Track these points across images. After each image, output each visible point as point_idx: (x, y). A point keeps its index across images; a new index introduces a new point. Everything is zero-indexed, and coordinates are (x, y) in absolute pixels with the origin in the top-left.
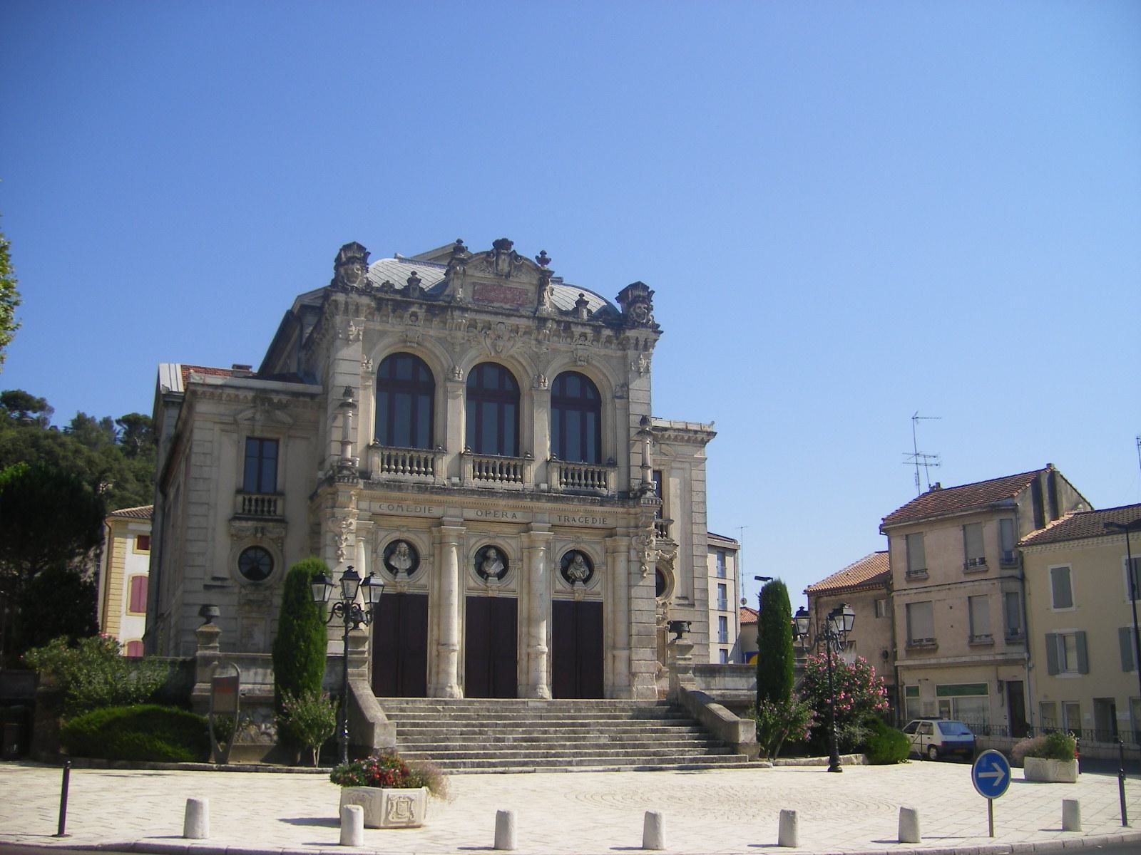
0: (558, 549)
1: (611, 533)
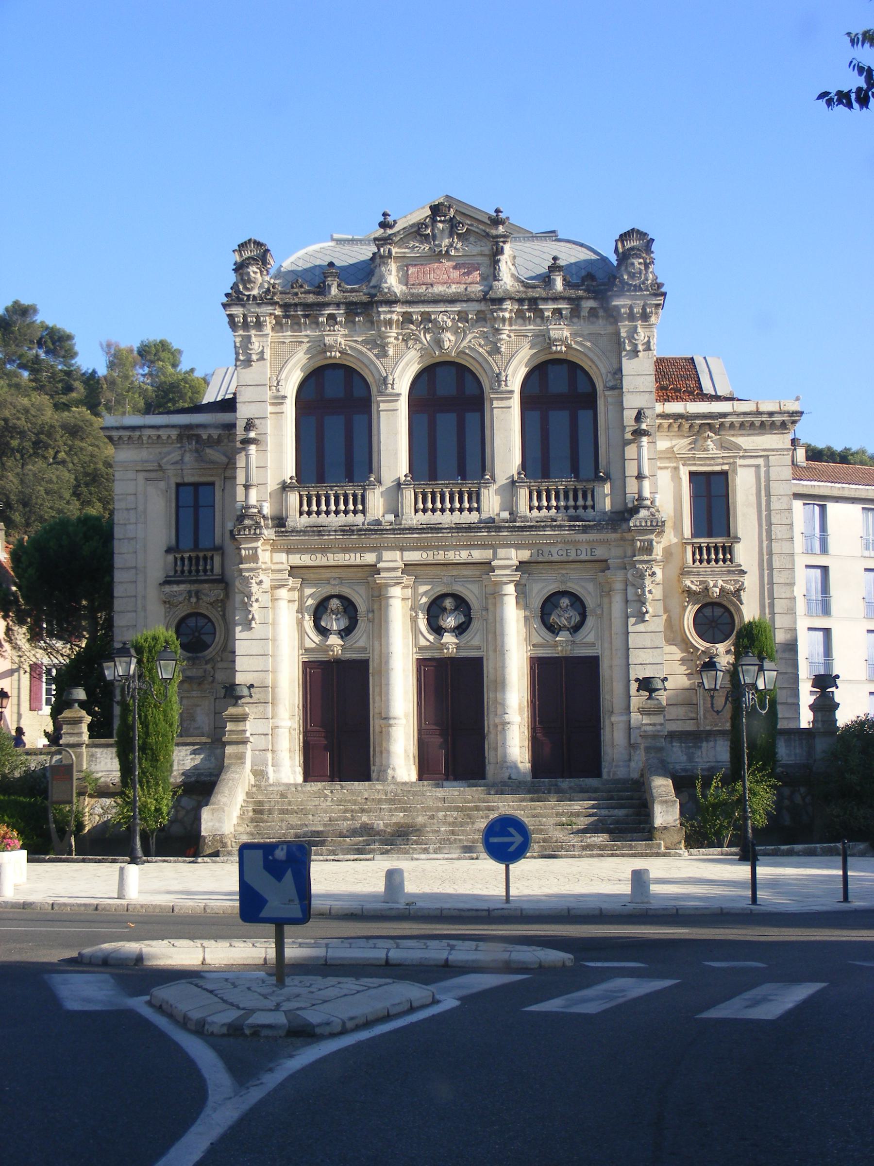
0: (535, 591)
1: (603, 565)
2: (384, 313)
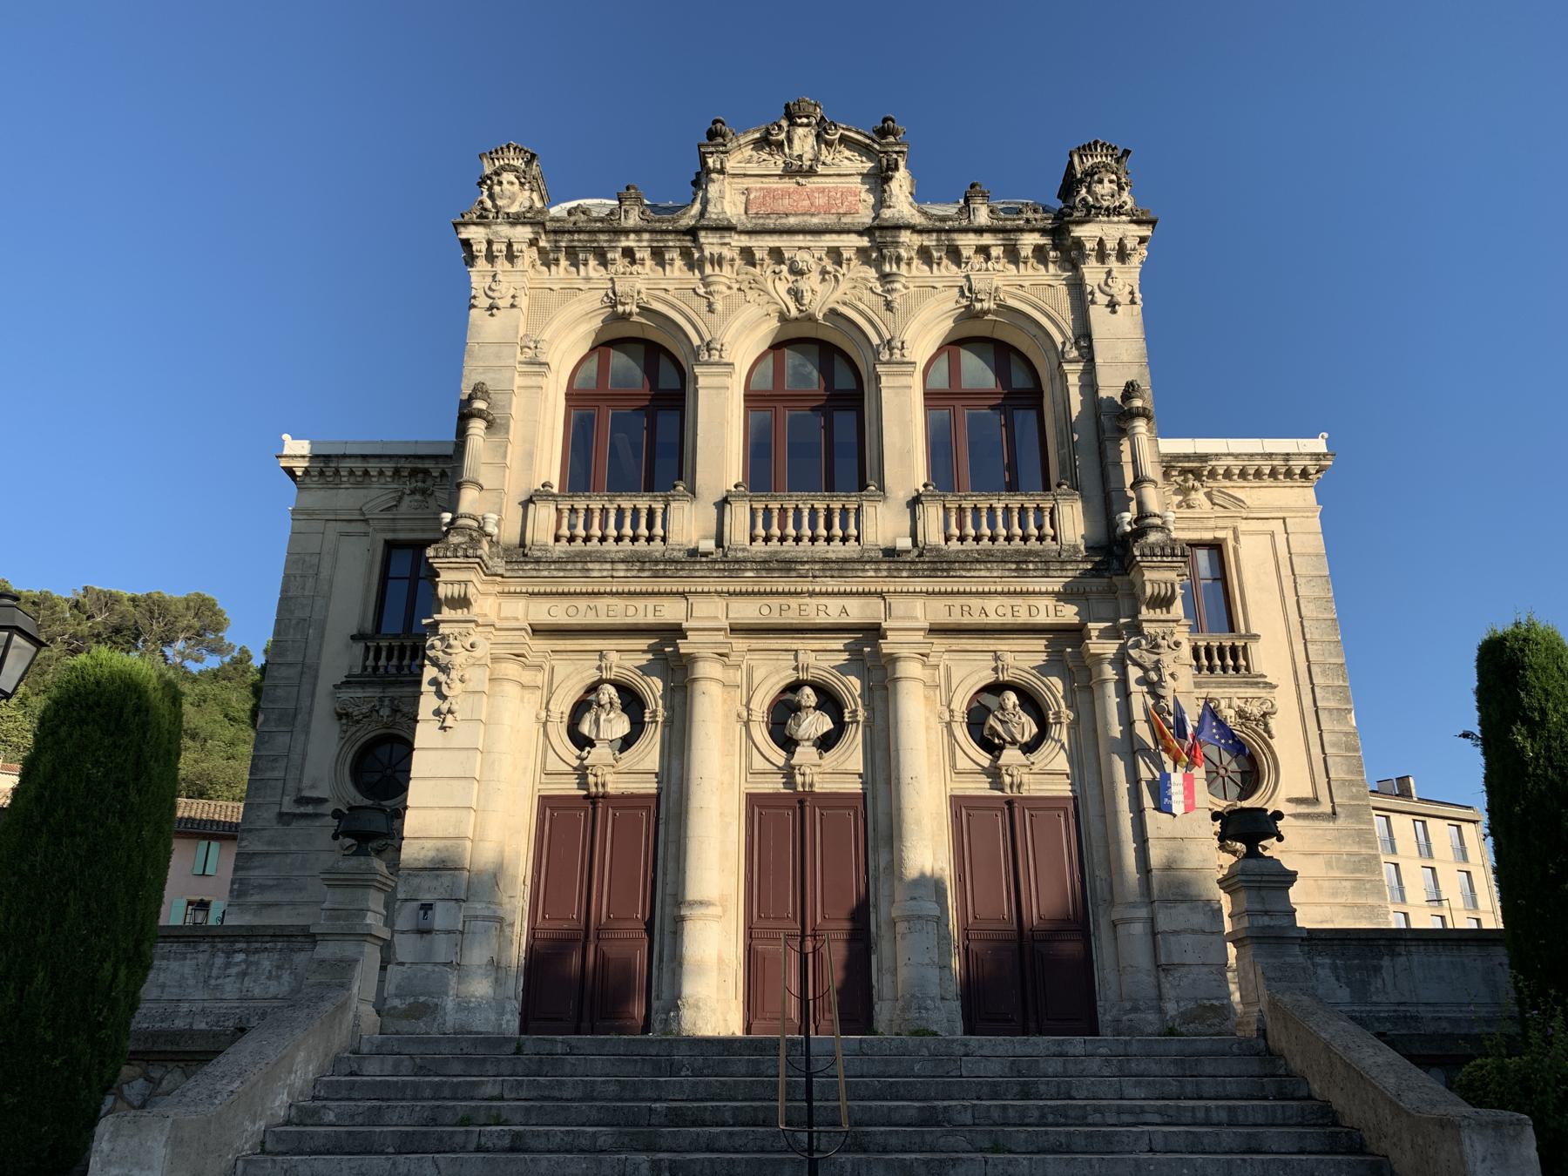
2: (710, 244)
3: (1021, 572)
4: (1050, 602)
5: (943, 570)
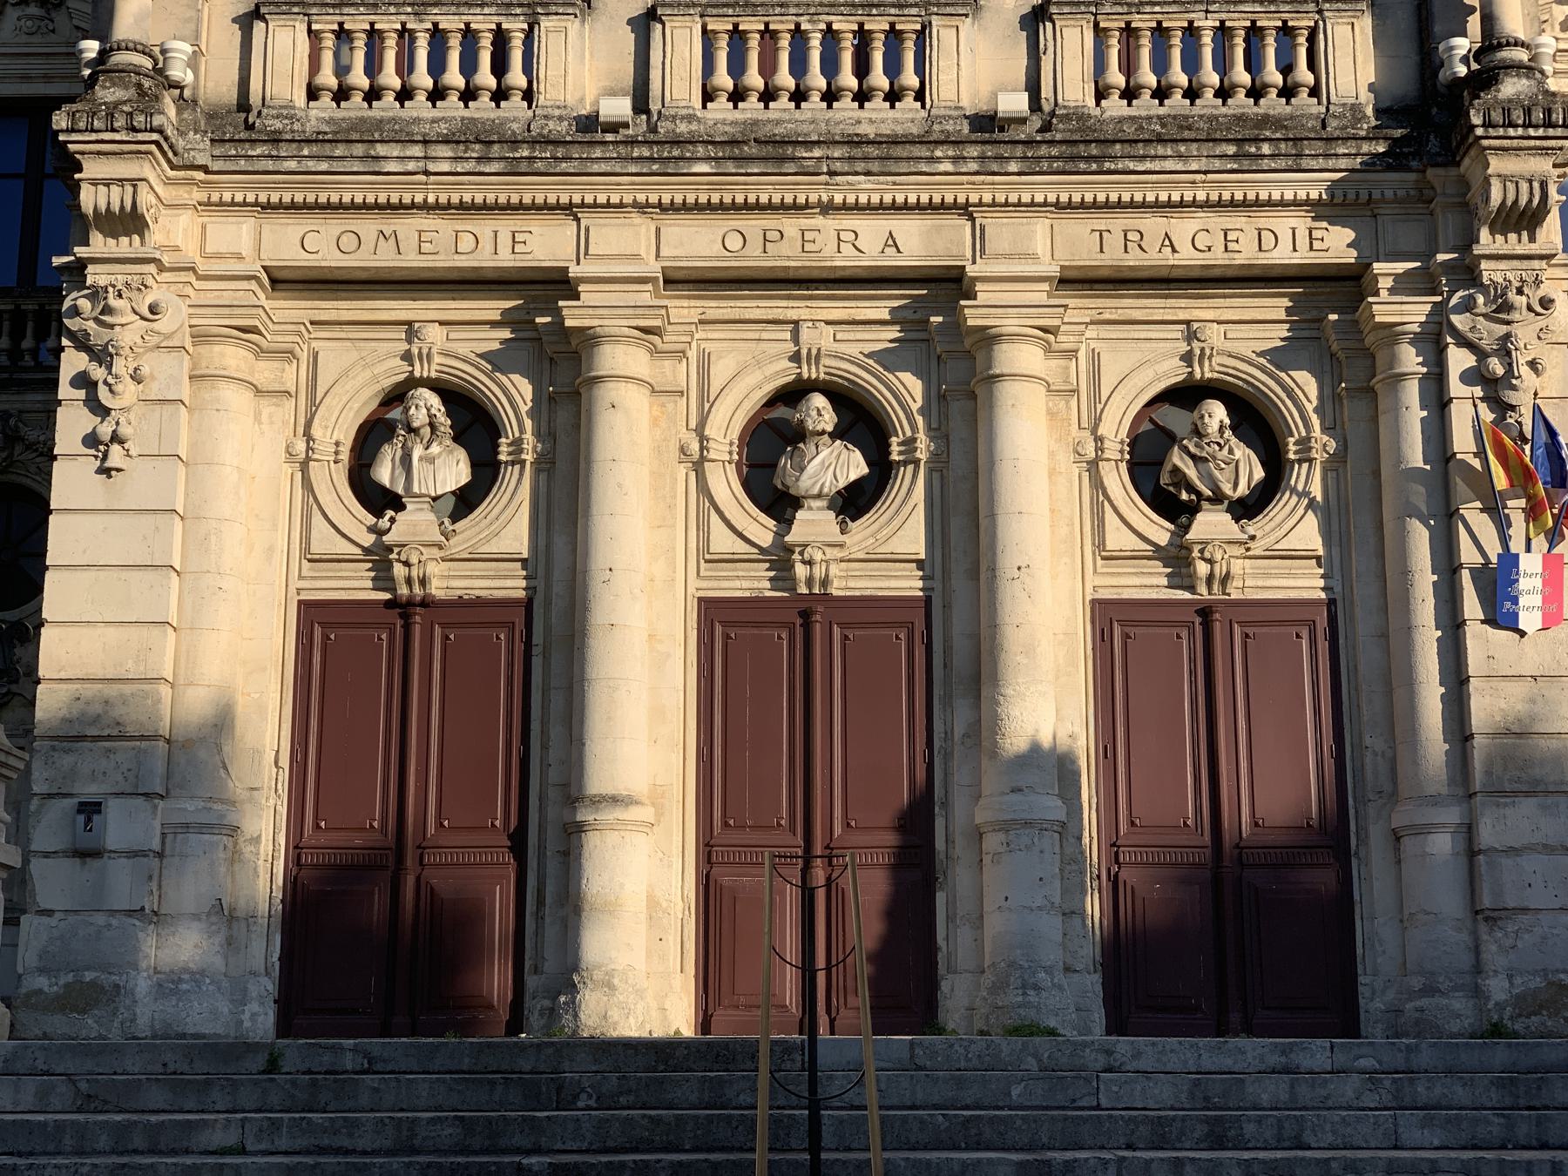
3: (1246, 160)
4: (1301, 222)
5: (1089, 158)
